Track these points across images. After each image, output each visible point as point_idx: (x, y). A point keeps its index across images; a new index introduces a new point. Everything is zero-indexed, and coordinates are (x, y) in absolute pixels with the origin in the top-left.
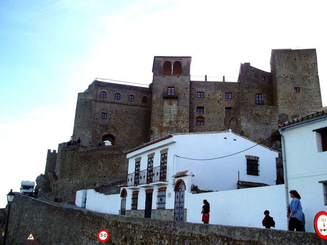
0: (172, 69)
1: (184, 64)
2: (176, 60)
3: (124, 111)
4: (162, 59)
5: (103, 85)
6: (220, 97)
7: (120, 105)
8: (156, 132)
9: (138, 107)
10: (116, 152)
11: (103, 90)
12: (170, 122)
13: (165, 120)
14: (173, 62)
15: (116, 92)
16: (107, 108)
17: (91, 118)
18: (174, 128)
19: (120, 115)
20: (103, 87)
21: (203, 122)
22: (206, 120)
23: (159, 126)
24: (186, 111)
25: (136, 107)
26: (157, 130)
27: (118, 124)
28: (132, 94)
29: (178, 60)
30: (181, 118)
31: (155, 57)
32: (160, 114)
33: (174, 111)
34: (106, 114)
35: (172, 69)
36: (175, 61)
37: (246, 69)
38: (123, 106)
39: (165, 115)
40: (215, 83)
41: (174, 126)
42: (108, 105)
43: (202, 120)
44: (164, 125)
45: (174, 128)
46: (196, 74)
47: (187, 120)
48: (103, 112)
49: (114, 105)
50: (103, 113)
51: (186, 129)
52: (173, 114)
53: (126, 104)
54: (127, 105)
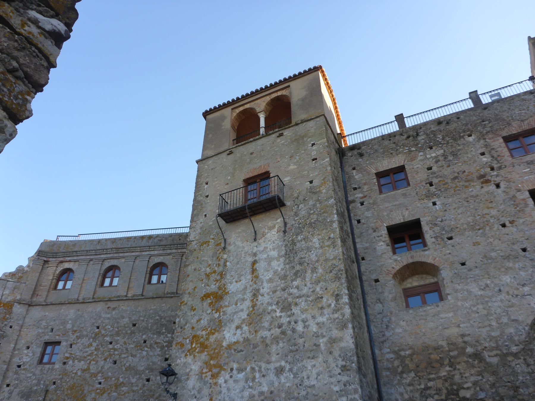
0: (262, 123)
1: (297, 93)
2: (274, 96)
4: (227, 112)
6: (485, 159)
7: (112, 305)
8: (192, 382)
11: (66, 265)
12: (255, 317)
13: (230, 310)
15: (107, 264)
16: (64, 323)
18: (276, 340)
19: (108, 339)
21: (436, 289)
22: (446, 274)
23: (204, 347)
24: (324, 248)
26: (195, 367)
27: (95, 375)
29: (279, 93)
30: (304, 286)
31: (206, 114)
32: (213, 287)
33: (269, 260)
35: (262, 123)
36: (268, 99)
38: (124, 306)
39: (232, 287)
41: (277, 331)
42: (71, 312)
43: (430, 280)
44: (229, 335)
45: (276, 340)
46: (362, 112)
47: (333, 286)
48: (47, 338)
49: (90, 308)
50: (47, 344)
51: (335, 333)
52: (270, 275)
53: (134, 299)
54: (142, 297)
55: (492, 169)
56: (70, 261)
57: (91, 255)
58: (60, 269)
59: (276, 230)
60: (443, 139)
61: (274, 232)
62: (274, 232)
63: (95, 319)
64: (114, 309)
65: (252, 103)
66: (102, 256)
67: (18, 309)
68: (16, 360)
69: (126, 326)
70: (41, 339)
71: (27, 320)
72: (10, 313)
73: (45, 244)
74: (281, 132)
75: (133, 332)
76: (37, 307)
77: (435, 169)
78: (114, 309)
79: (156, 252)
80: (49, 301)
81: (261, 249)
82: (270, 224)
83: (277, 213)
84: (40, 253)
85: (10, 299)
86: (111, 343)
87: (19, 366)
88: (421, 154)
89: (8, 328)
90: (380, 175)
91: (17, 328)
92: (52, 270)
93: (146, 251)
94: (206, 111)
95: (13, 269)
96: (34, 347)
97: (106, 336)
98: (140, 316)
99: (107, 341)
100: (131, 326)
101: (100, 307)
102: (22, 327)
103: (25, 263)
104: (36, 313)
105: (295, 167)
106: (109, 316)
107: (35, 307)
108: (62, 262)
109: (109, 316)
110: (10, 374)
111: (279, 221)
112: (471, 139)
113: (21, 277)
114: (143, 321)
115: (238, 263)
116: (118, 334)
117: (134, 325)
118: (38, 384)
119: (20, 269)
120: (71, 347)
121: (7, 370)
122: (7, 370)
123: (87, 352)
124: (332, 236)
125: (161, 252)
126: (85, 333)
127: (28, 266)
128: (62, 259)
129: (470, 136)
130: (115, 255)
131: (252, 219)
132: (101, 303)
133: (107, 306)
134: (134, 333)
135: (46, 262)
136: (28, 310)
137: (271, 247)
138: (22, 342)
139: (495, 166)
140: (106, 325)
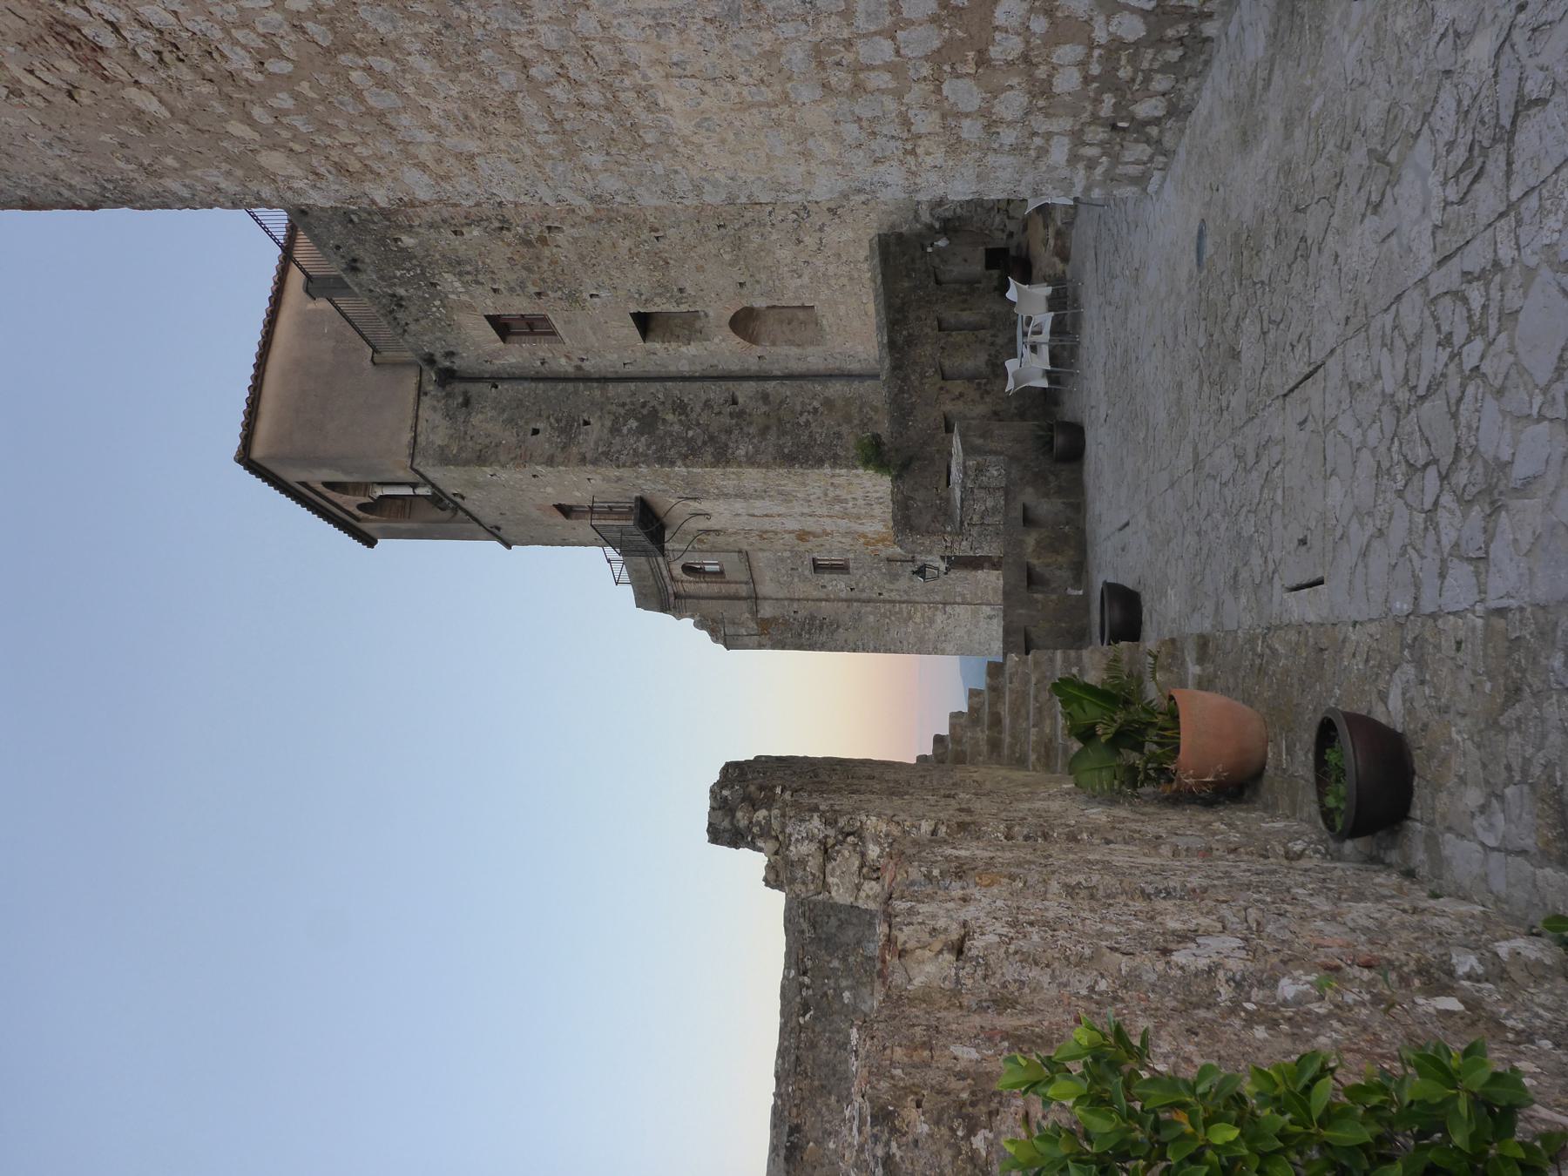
11: (677, 570)
17: (858, 618)
56: (670, 571)
58: (685, 577)
67: (767, 611)
68: (843, 595)
71: (781, 595)
72: (775, 619)
73: (643, 601)
80: (744, 577)
84: (664, 608)
85: (753, 625)
89: (798, 616)
91: (796, 606)
92: (690, 585)
95: (705, 634)
102: (792, 600)
103: (688, 622)
104: (767, 588)
108: (672, 578)
110: (864, 596)
113: (713, 620)
118: (879, 569)
119: (700, 625)
121: (858, 600)
122: (858, 600)
127: (692, 616)
128: (667, 580)
135: (677, 596)
136: (765, 598)
138: (815, 594)
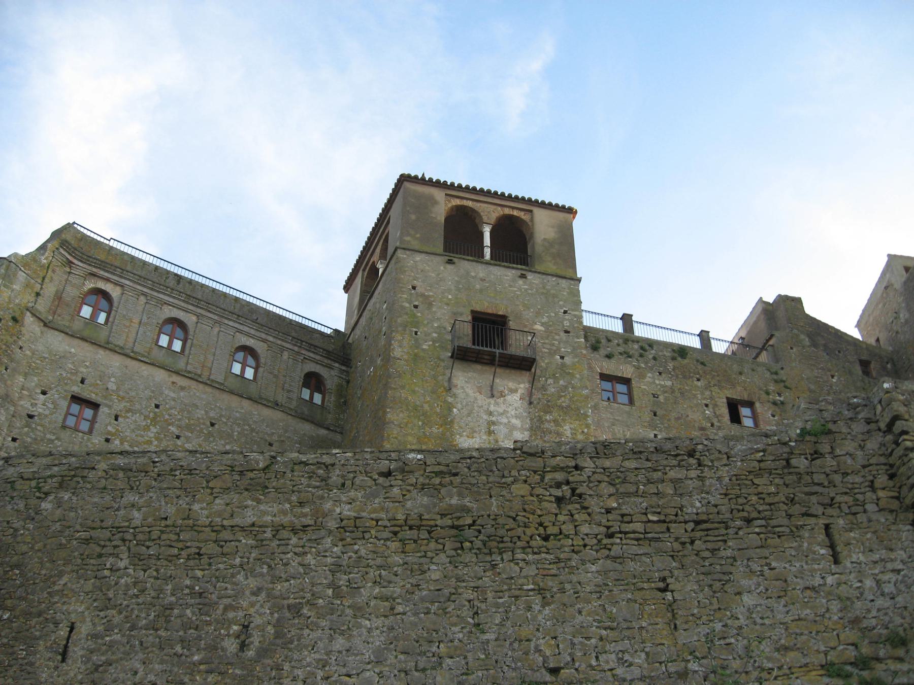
0: (487, 240)
2: (507, 211)
3: (200, 413)
4: (439, 195)
5: (102, 257)
9: (277, 415)
10: (268, 511)
11: (101, 285)
14: (490, 214)
20: (103, 265)
25: (267, 412)
28: (250, 342)
29: (515, 213)
33: (513, 428)
34: (95, 406)
35: (487, 240)
36: (500, 212)
37: (781, 319)
40: (682, 351)
48: (76, 389)
49: (146, 370)
50: (76, 399)
55: (712, 425)
57: (144, 286)
59: (518, 395)
60: (673, 370)
61: (516, 397)
62: (516, 397)
63: (153, 392)
64: (182, 388)
65: (479, 204)
66: (161, 296)
69: (201, 421)
70: (67, 388)
74: (524, 272)
75: (210, 434)
76: (57, 333)
77: (661, 398)
78: (182, 388)
79: (246, 329)
81: (501, 410)
82: (511, 385)
83: (526, 376)
86: (178, 437)
87: (31, 417)
88: (649, 375)
90: (604, 377)
93: (230, 320)
94: (409, 176)
96: (53, 394)
97: (172, 424)
98: (221, 416)
99: (173, 432)
100: (209, 423)
101: (160, 375)
104: (57, 342)
105: (543, 329)
106: (173, 395)
107: (52, 331)
109: (173, 395)
111: (522, 386)
112: (699, 384)
114: (226, 423)
115: (469, 415)
116: (189, 427)
117: (212, 425)
120: (116, 419)
123: (142, 436)
124: (586, 430)
125: (252, 332)
126: (137, 406)
128: (94, 270)
129: (698, 380)
130: (183, 304)
131: (498, 370)
132: (162, 371)
133: (171, 380)
134: (213, 436)
137: (513, 413)
139: (716, 424)
140: (171, 409)
